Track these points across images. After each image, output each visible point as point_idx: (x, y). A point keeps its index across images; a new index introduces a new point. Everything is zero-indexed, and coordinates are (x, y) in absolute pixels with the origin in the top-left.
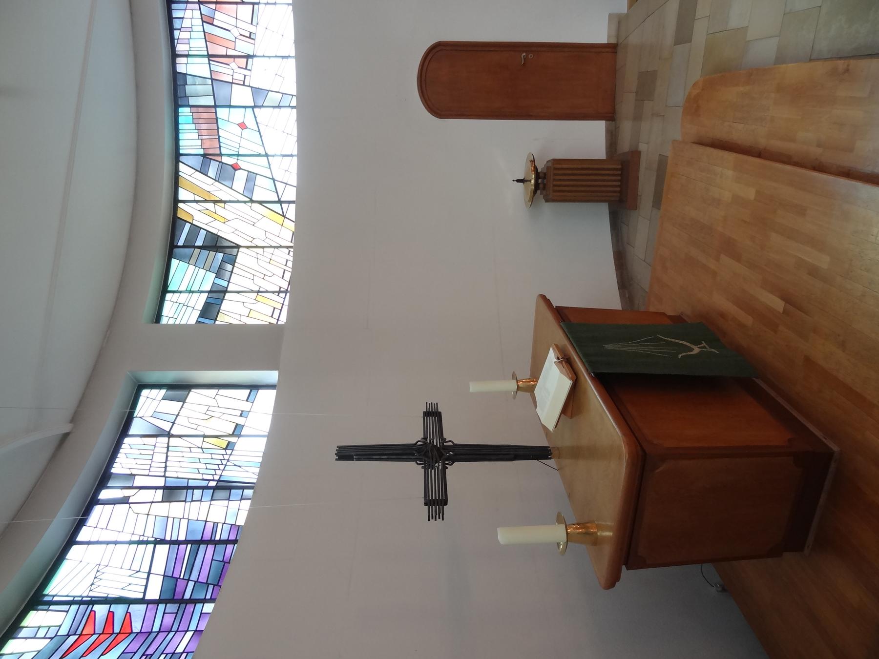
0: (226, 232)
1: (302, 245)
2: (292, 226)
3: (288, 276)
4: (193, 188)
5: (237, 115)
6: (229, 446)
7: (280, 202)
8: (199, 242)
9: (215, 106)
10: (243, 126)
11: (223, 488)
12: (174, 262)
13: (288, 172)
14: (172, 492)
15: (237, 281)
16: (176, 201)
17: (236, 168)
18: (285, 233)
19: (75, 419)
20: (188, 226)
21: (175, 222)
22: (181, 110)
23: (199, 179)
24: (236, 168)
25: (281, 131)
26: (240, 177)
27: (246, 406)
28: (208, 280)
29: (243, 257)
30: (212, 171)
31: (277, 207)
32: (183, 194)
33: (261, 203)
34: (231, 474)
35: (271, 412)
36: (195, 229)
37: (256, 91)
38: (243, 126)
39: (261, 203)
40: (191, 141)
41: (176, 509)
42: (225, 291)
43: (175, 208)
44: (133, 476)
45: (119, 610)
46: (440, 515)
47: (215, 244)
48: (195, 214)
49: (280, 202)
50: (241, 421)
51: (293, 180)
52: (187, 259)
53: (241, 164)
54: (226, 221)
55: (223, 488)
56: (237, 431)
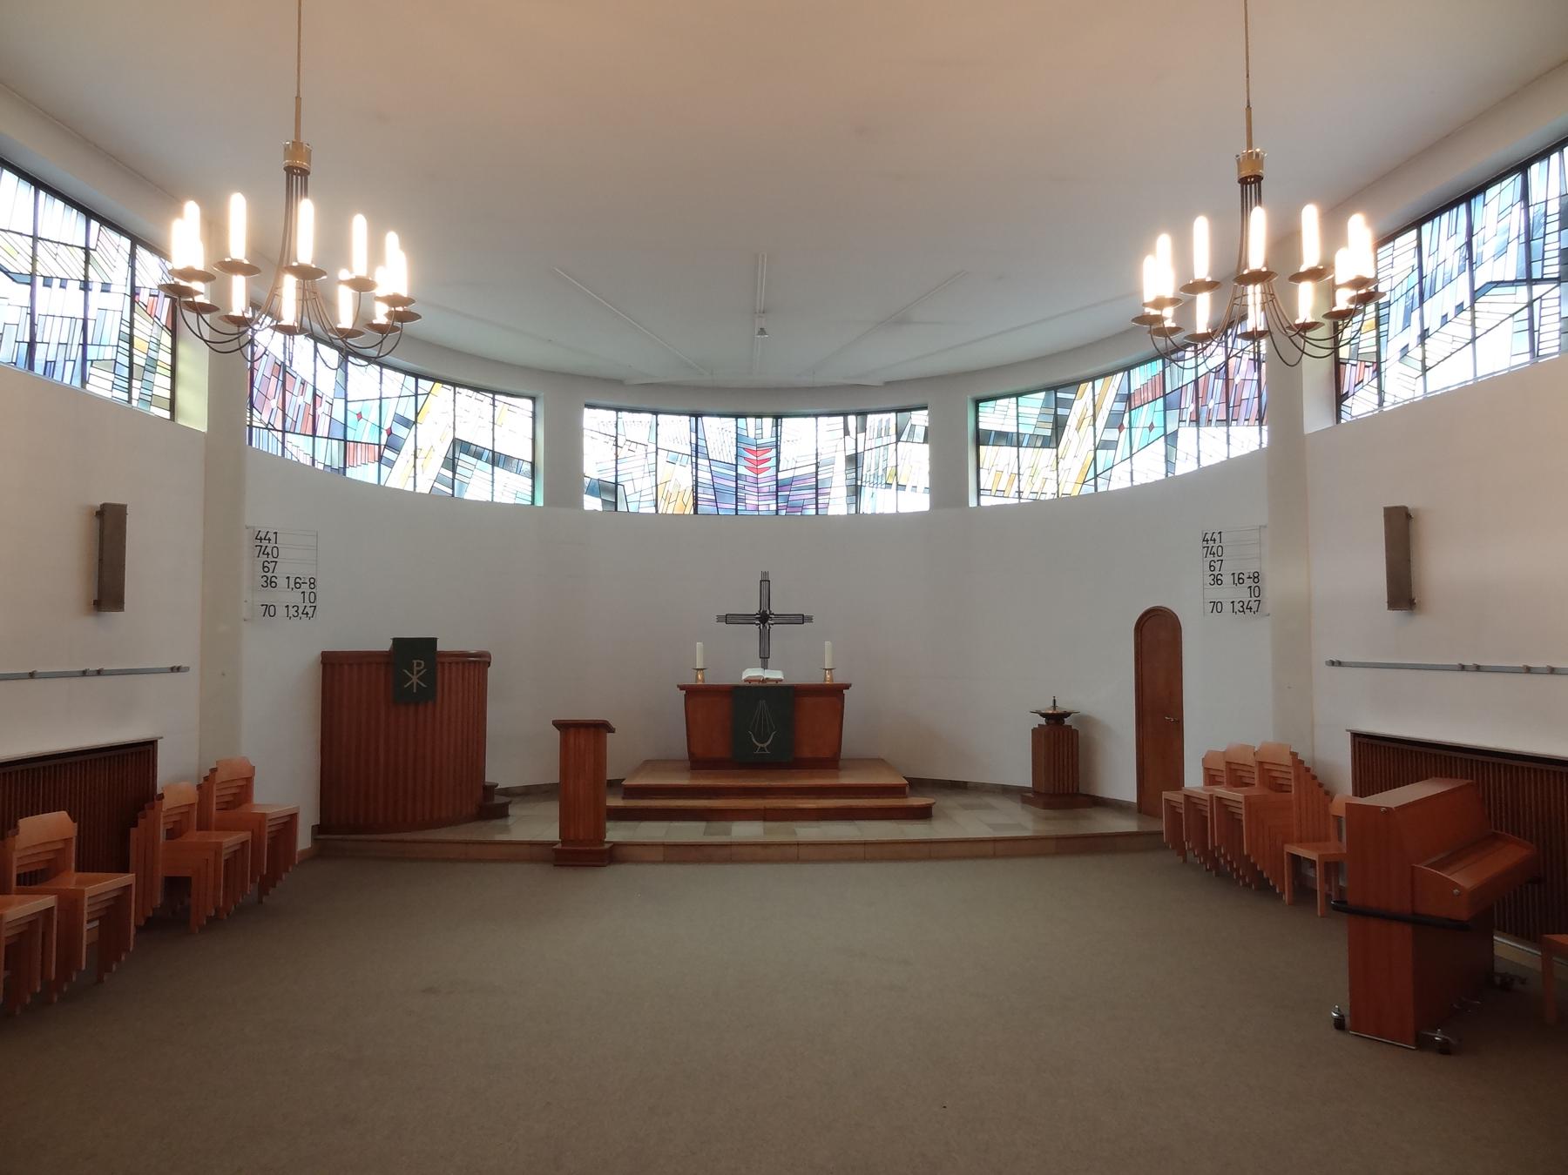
0: (1069, 433)
1: (1062, 506)
2: (1075, 493)
3: (1033, 496)
4: (1104, 394)
5: (1158, 422)
6: (889, 485)
7: (1096, 476)
8: (1060, 411)
9: (1165, 395)
10: (1151, 427)
11: (856, 491)
12: (1042, 395)
13: (1119, 481)
14: (854, 461)
15: (1026, 453)
16: (1093, 379)
17: (1121, 428)
18: (1070, 488)
19: (888, 383)
20: (1071, 396)
21: (1073, 385)
22: (1160, 362)
23: (1111, 395)
24: (1121, 428)
25: (1149, 468)
26: (1112, 435)
27: (921, 488)
28: (1026, 430)
29: (1048, 453)
30: (1120, 406)
31: (1091, 475)
32: (1098, 383)
33: (1095, 459)
34: (866, 492)
35: (901, 510)
36: (1069, 404)
37: (1175, 433)
38: (1151, 427)
39: (1095, 459)
40: (1140, 376)
41: (841, 464)
42: (1019, 445)
43: (1086, 380)
44: (864, 430)
45: (773, 462)
46: (719, 619)
47: (1059, 425)
48: (1081, 403)
49: (1096, 476)
50: (908, 488)
51: (1114, 486)
52: (1046, 405)
53: (1125, 432)
54: (1078, 429)
55: (856, 491)
56: (900, 487)
